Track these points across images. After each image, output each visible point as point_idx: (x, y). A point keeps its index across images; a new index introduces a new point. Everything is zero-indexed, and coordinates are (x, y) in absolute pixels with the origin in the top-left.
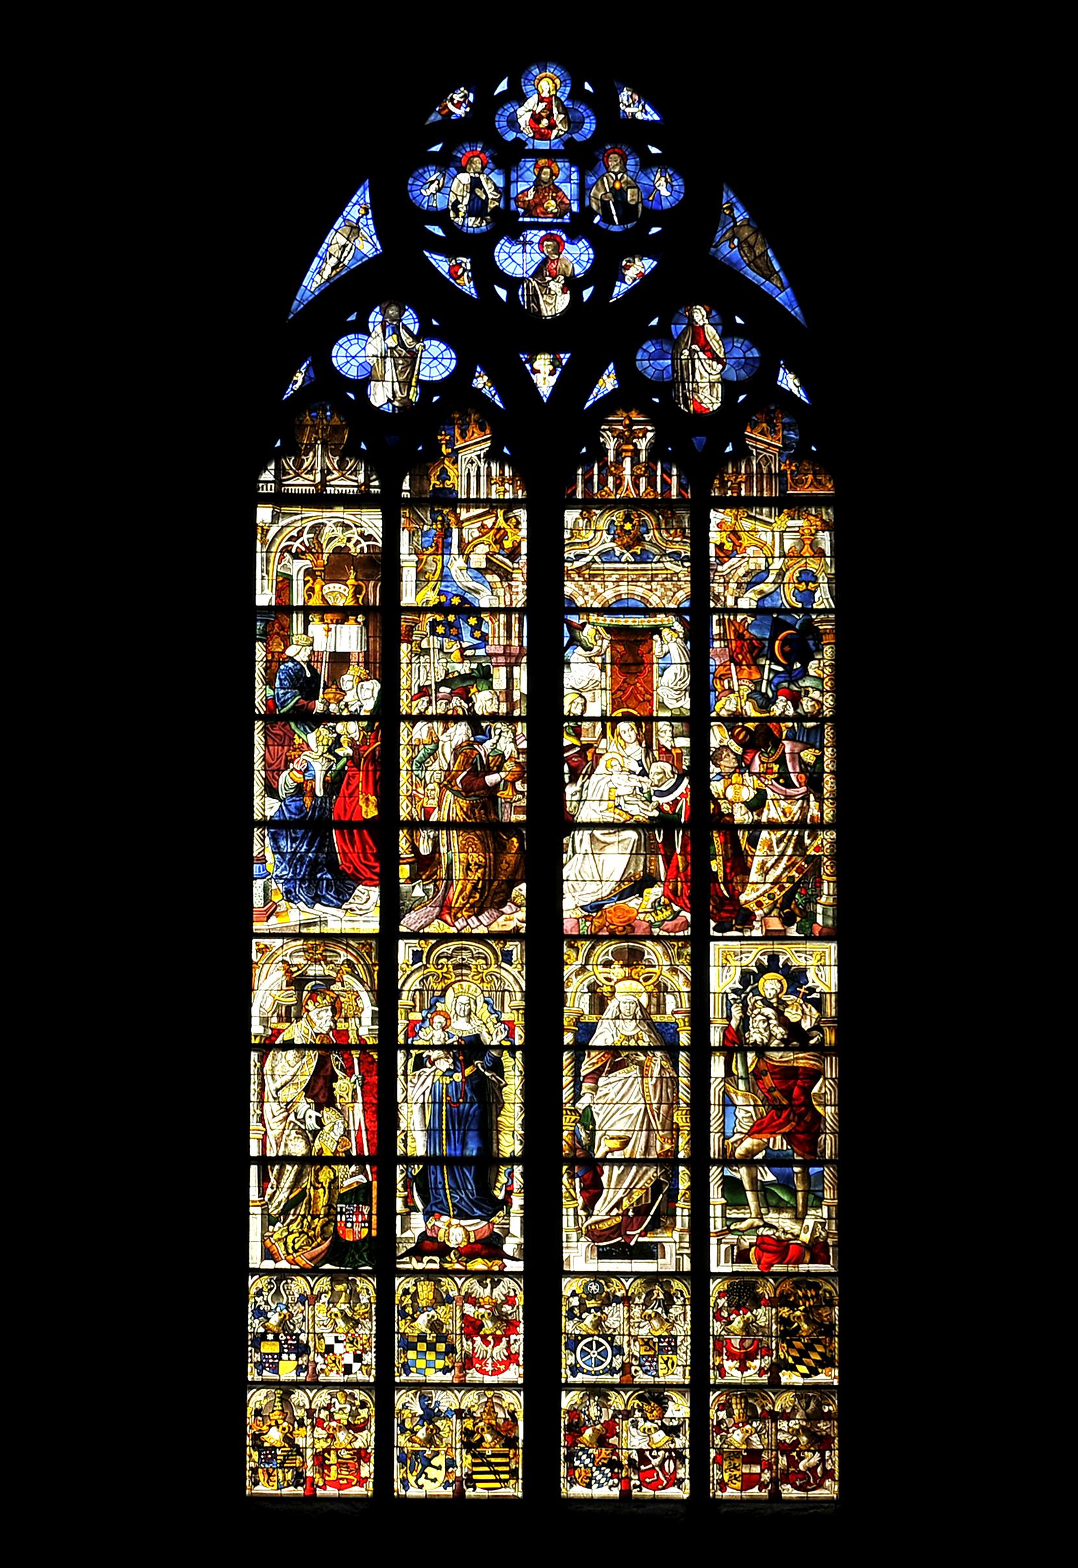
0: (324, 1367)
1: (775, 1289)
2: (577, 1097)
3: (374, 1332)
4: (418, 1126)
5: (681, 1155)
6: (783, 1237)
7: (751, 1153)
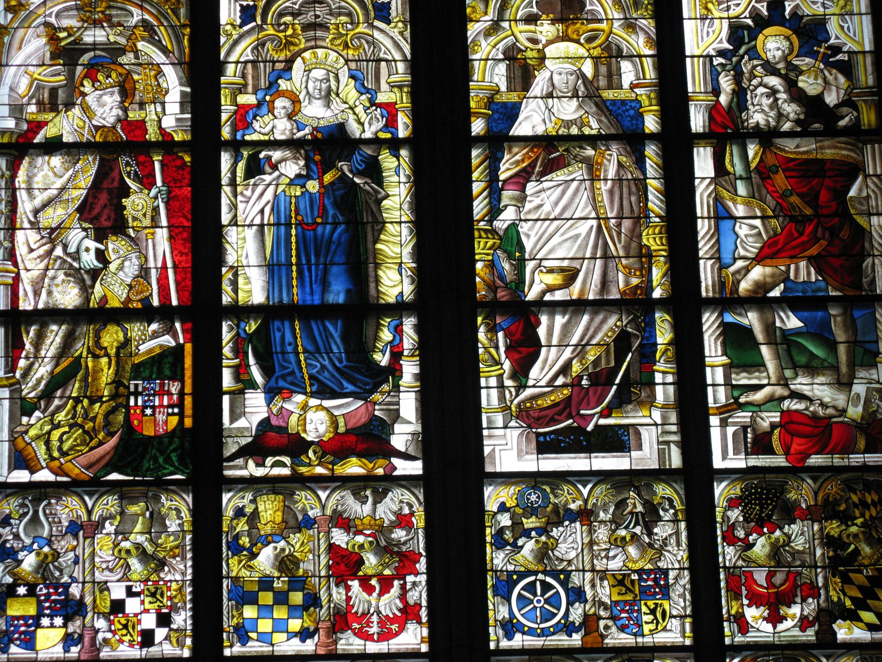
0: (109, 635)
1: (816, 494)
2: (494, 211)
3: (189, 577)
4: (254, 259)
5: (657, 294)
6: (821, 412)
7: (762, 287)
